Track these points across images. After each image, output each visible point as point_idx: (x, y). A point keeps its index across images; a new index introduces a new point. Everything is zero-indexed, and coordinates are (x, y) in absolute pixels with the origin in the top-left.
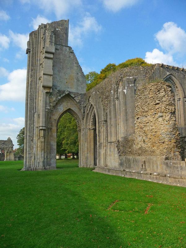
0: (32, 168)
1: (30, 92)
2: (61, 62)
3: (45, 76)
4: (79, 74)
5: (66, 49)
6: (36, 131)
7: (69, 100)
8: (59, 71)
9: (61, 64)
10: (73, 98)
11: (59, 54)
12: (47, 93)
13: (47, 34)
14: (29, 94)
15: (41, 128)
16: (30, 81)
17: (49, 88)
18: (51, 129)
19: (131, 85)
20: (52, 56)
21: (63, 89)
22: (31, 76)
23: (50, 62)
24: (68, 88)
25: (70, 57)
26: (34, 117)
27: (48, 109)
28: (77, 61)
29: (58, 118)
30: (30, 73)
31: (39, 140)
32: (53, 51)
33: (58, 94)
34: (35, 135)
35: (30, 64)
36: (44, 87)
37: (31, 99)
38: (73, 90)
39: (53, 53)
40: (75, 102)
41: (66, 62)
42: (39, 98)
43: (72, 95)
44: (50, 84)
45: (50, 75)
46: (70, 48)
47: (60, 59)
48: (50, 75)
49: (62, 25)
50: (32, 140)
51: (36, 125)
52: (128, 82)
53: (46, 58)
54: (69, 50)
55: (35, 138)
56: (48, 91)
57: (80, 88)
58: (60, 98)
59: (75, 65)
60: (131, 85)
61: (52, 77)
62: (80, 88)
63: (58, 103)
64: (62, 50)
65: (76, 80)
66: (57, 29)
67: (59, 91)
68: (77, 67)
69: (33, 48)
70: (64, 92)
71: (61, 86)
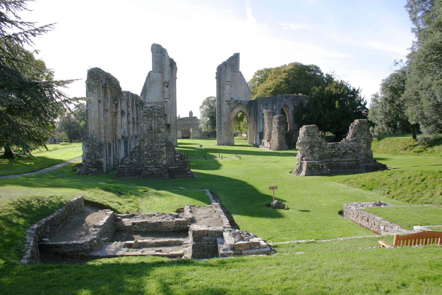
3: (226, 95)
5: (238, 74)
6: (223, 125)
12: (228, 104)
20: (229, 83)
23: (229, 86)
36: (226, 101)
38: (243, 99)
44: (229, 99)
46: (240, 73)
51: (223, 121)
56: (228, 103)
59: (244, 83)
67: (235, 101)
70: (238, 101)
71: (236, 98)
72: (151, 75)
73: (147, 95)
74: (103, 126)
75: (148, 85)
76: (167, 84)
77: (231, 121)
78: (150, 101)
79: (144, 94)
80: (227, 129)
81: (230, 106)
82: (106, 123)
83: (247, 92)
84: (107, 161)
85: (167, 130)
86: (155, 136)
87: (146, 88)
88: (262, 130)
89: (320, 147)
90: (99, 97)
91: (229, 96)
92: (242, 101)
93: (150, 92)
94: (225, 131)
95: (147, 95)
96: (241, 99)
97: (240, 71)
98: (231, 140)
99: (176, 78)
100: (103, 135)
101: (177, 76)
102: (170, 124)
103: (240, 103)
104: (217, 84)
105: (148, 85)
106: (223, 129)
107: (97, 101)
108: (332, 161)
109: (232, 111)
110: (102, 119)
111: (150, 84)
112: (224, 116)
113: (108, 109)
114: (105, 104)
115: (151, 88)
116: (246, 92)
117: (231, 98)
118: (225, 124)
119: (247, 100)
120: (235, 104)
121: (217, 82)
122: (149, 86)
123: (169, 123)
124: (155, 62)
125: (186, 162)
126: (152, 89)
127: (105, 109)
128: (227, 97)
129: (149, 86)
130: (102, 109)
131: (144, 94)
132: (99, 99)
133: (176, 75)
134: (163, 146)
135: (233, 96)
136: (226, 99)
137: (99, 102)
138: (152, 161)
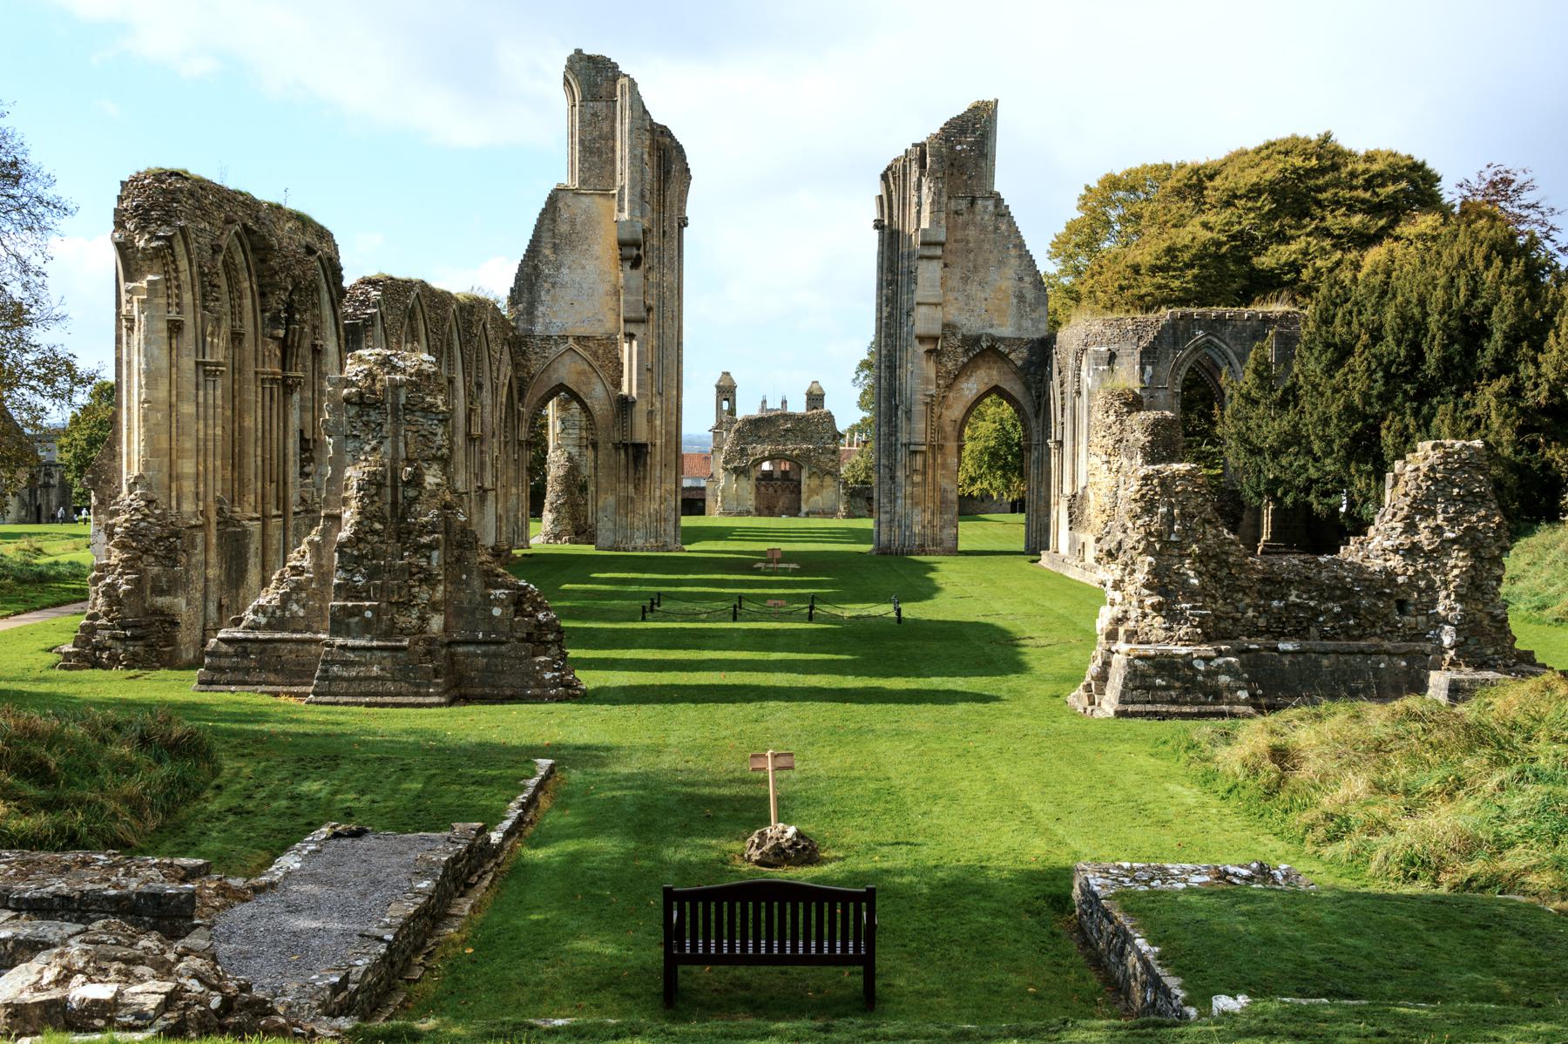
0: (893, 548)
1: (886, 346)
2: (970, 251)
4: (1027, 279)
5: (986, 207)
7: (996, 362)
8: (965, 280)
9: (971, 256)
10: (1007, 356)
11: (966, 226)
12: (929, 352)
13: (925, 190)
14: (883, 352)
15: (912, 448)
16: (885, 314)
17: (935, 339)
18: (941, 447)
19: (1101, 368)
20: (938, 252)
21: (975, 331)
22: (887, 300)
23: (936, 266)
24: (991, 326)
25: (997, 228)
26: (896, 415)
27: (932, 396)
28: (1019, 237)
29: (961, 417)
30: (884, 291)
31: (909, 481)
32: (942, 238)
33: (959, 350)
34: (899, 466)
35: (885, 266)
36: (922, 339)
37: (888, 367)
38: (1006, 330)
39: (942, 244)
40: (1012, 366)
41: (986, 246)
42: (909, 365)
43: (1002, 348)
44: (936, 330)
45: (936, 305)
46: (998, 200)
47: (968, 242)
48: (936, 305)
49: (976, 120)
50: (893, 478)
52: (1095, 359)
53: (921, 257)
54: (996, 207)
55: (899, 474)
56: (932, 347)
57: (1027, 324)
58: (965, 360)
59: (1013, 252)
60: (1101, 368)
61: (939, 308)
62: (1027, 324)
63: (963, 371)
64: (974, 213)
65: (1015, 301)
66: (958, 148)
67: (965, 339)
68: (1020, 256)
69: (891, 216)
70: (978, 339)
71: (971, 324)
72: (561, 205)
73: (542, 303)
74: (189, 444)
75: (547, 252)
76: (635, 252)
77: (945, 438)
78: (554, 332)
79: (526, 295)
80: (924, 473)
81: (939, 363)
82: (210, 432)
83: (1030, 295)
84: (205, 607)
85: (631, 471)
86: (395, 496)
87: (536, 267)
88: (1084, 484)
89: (1213, 576)
90: (174, 309)
91: (938, 313)
92: (1002, 339)
93: (554, 285)
94: (914, 484)
95: (542, 303)
96: (998, 332)
97: (996, 188)
98: (942, 528)
99: (683, 223)
100: (188, 486)
101: (690, 211)
102: (645, 445)
103: (992, 349)
104: (881, 253)
105: (547, 252)
106: (900, 474)
107: (164, 325)
108: (1276, 649)
109: (949, 387)
110: (188, 409)
111: (555, 248)
112: (908, 412)
113: (217, 364)
114: (204, 341)
115: (558, 268)
116: (1021, 298)
117: (946, 326)
118: (915, 452)
119: (1026, 336)
120: (966, 352)
121: (882, 241)
122: (552, 257)
123: (641, 435)
124: (581, 142)
125: (539, 625)
126: (565, 270)
127: (205, 364)
128: (925, 321)
129: (552, 257)
130: (188, 363)
131: (526, 295)
132: (173, 316)
133: (682, 209)
134: (430, 547)
135: (953, 314)
136: (921, 327)
137: (169, 329)
138: (368, 614)
